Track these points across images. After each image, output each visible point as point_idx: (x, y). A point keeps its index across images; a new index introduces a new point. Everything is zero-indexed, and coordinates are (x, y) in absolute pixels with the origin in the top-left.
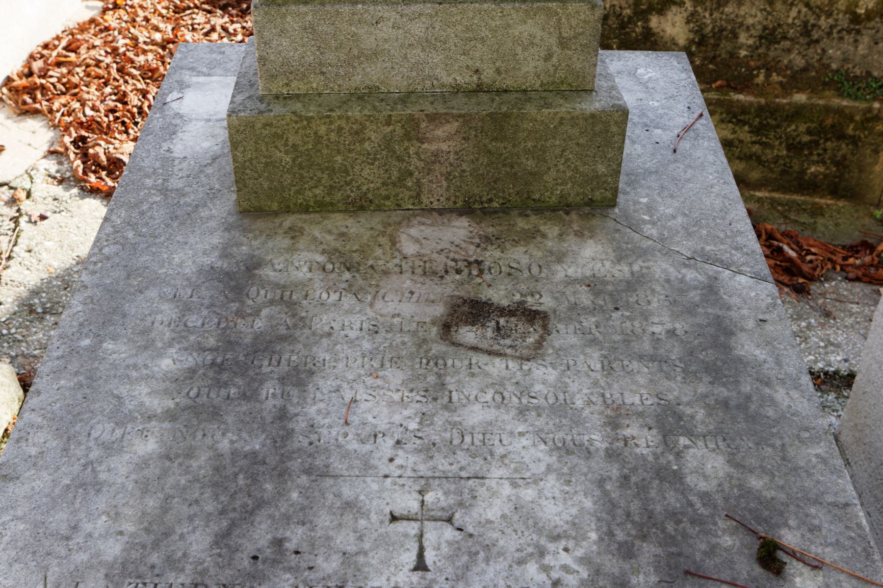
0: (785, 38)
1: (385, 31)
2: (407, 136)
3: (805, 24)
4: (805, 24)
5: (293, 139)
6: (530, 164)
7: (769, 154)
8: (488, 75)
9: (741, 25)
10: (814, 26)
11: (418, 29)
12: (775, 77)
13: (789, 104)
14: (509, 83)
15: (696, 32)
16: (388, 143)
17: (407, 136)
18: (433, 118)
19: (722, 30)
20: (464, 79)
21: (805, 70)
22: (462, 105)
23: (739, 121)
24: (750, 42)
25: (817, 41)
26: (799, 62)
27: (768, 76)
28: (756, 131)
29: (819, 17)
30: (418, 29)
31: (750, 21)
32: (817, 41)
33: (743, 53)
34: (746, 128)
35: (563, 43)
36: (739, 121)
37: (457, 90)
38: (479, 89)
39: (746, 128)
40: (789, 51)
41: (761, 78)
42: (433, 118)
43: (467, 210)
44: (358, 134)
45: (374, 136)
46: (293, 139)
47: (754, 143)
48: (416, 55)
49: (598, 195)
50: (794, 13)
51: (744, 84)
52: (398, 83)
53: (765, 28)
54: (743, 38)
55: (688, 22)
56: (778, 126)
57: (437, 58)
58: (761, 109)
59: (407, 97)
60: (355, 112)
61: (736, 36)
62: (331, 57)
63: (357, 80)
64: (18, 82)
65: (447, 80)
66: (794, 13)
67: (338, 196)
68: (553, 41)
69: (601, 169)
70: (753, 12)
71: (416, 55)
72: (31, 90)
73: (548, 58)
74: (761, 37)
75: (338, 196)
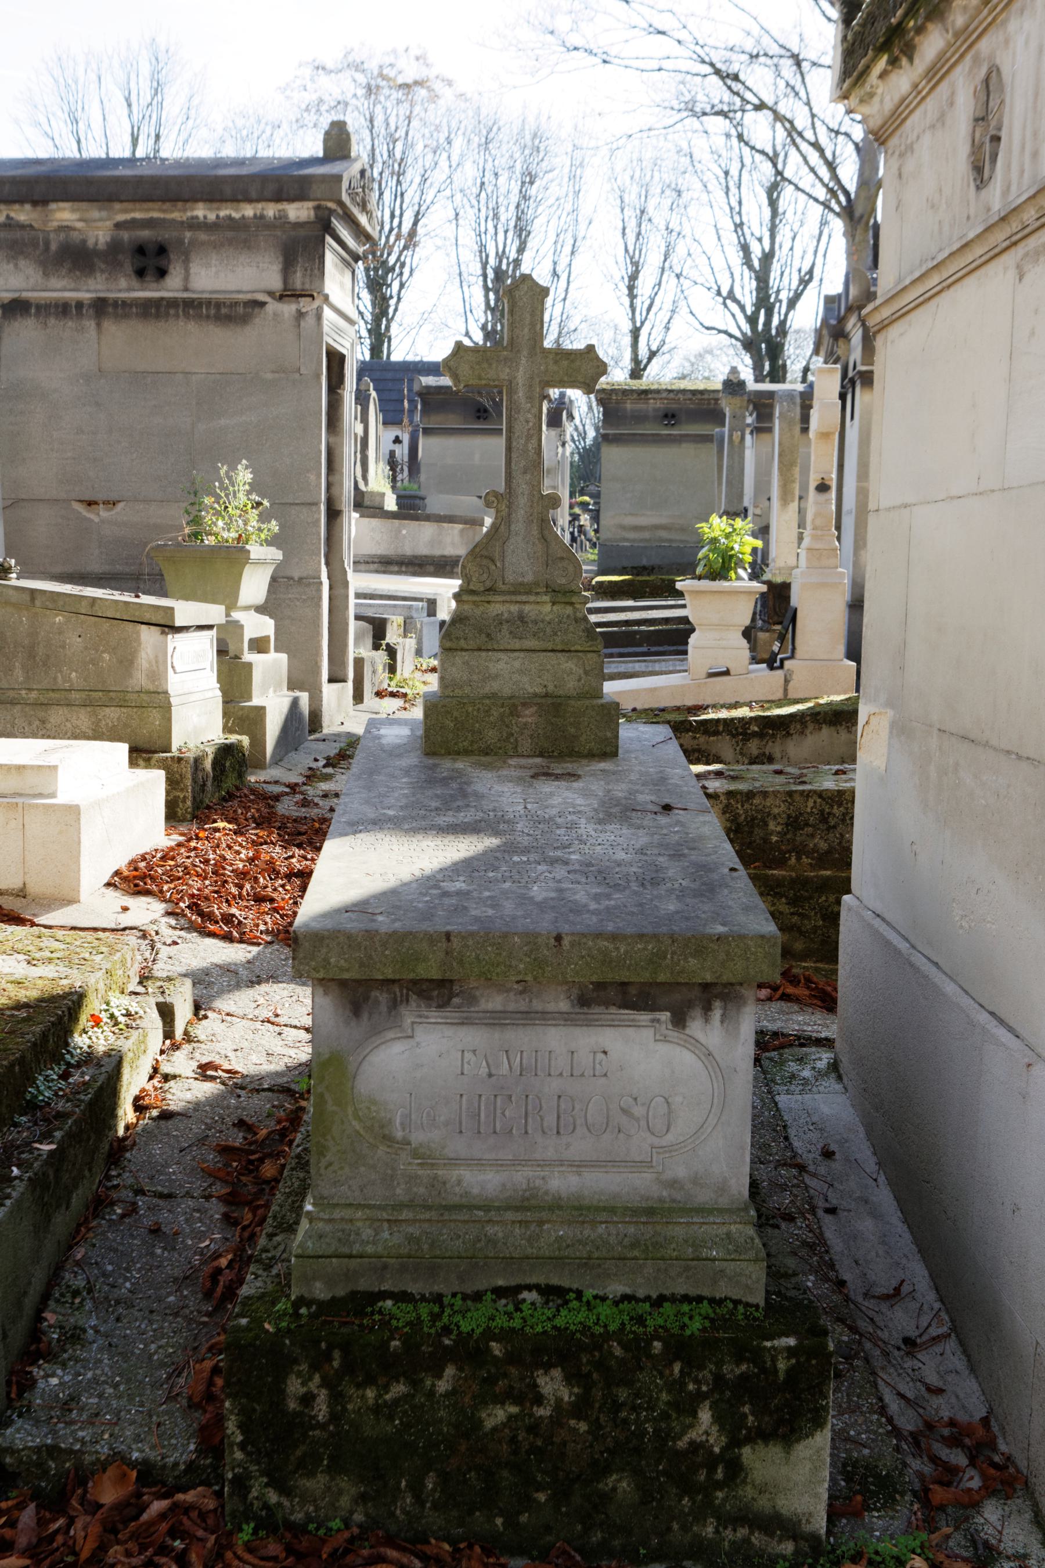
0: (807, 825)
1: (501, 665)
2: (511, 714)
3: (822, 811)
4: (822, 811)
5: (456, 714)
6: (573, 730)
7: (808, 925)
8: (551, 688)
9: (769, 814)
10: (829, 814)
11: (517, 664)
12: (805, 860)
13: (816, 876)
14: (561, 692)
15: (732, 821)
16: (502, 716)
17: (511, 714)
18: (524, 704)
19: (753, 819)
20: (539, 690)
21: (828, 852)
22: (539, 700)
23: (776, 894)
24: (779, 829)
25: (834, 827)
26: (823, 846)
27: (799, 859)
28: (793, 902)
29: (832, 807)
30: (517, 664)
31: (776, 811)
32: (834, 827)
33: (774, 839)
34: (784, 900)
35: (586, 673)
36: (776, 894)
37: (536, 695)
38: (546, 695)
39: (784, 900)
40: (812, 836)
41: (793, 860)
42: (524, 704)
43: (541, 755)
44: (487, 712)
45: (495, 713)
46: (456, 714)
47: (792, 914)
48: (516, 677)
49: (608, 750)
50: (810, 803)
51: (781, 863)
52: (507, 691)
53: (789, 817)
54: (772, 825)
55: (724, 813)
56: (811, 898)
57: (525, 679)
58: (793, 881)
59: (511, 698)
60: (487, 701)
61: (766, 824)
62: (475, 677)
63: (487, 690)
64: (126, 873)
65: (531, 691)
66: (810, 803)
67: (475, 746)
68: (581, 671)
69: (609, 734)
70: (777, 802)
71: (516, 677)
72: (143, 878)
73: (579, 680)
74: (787, 825)
75: (475, 746)
